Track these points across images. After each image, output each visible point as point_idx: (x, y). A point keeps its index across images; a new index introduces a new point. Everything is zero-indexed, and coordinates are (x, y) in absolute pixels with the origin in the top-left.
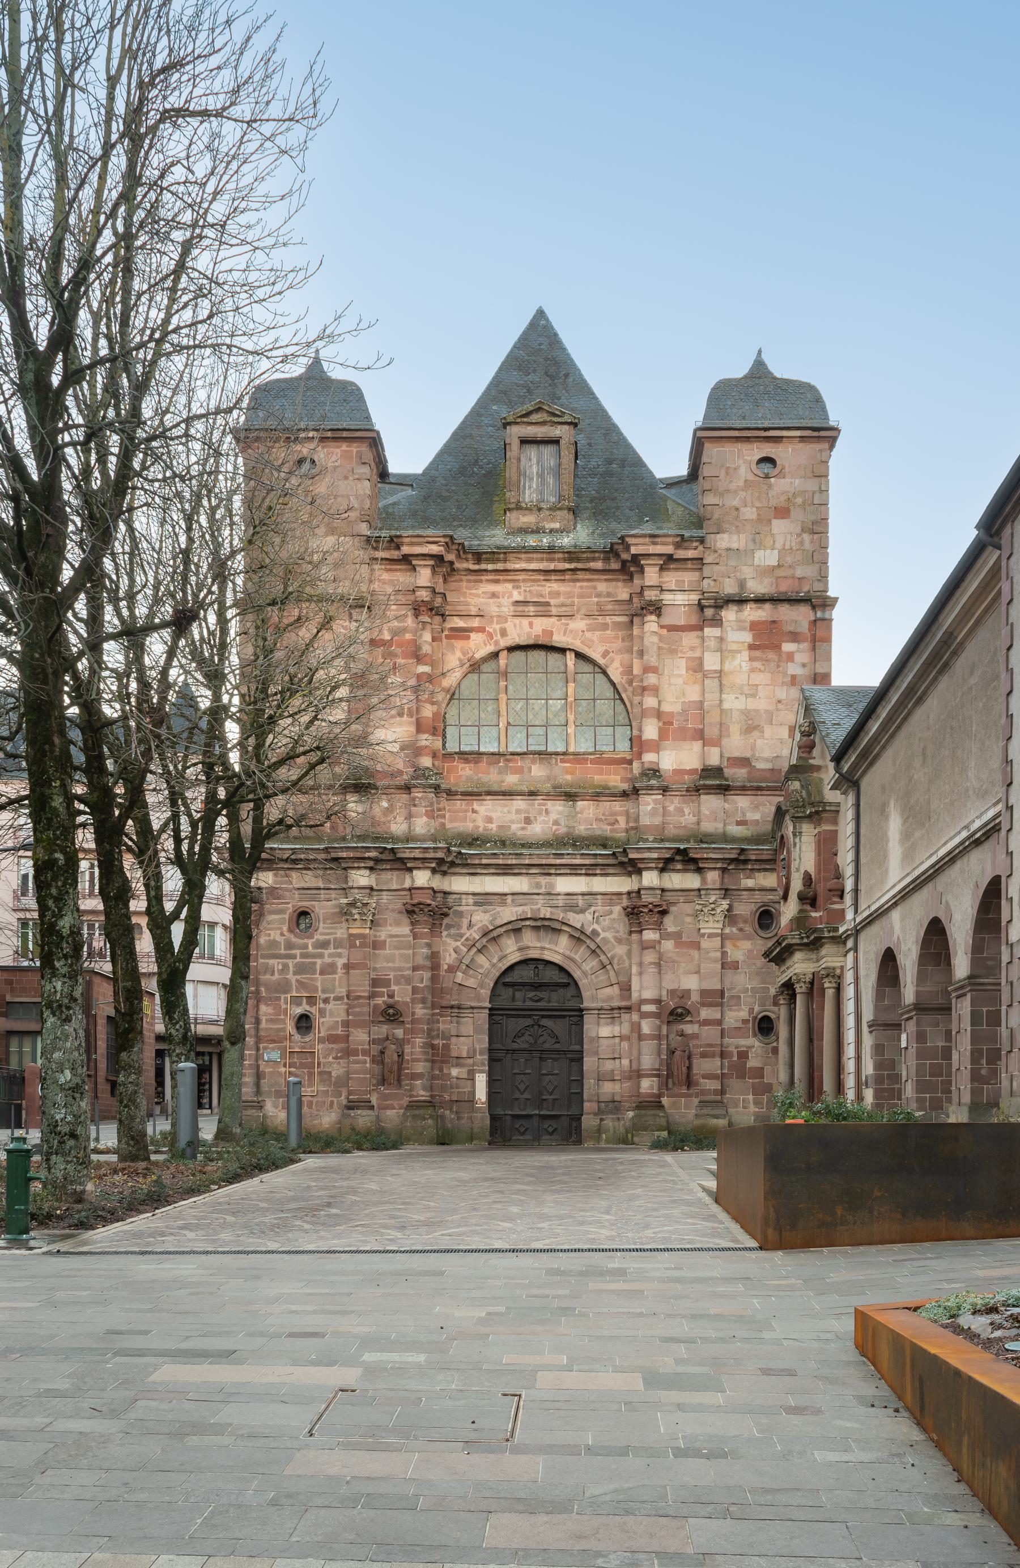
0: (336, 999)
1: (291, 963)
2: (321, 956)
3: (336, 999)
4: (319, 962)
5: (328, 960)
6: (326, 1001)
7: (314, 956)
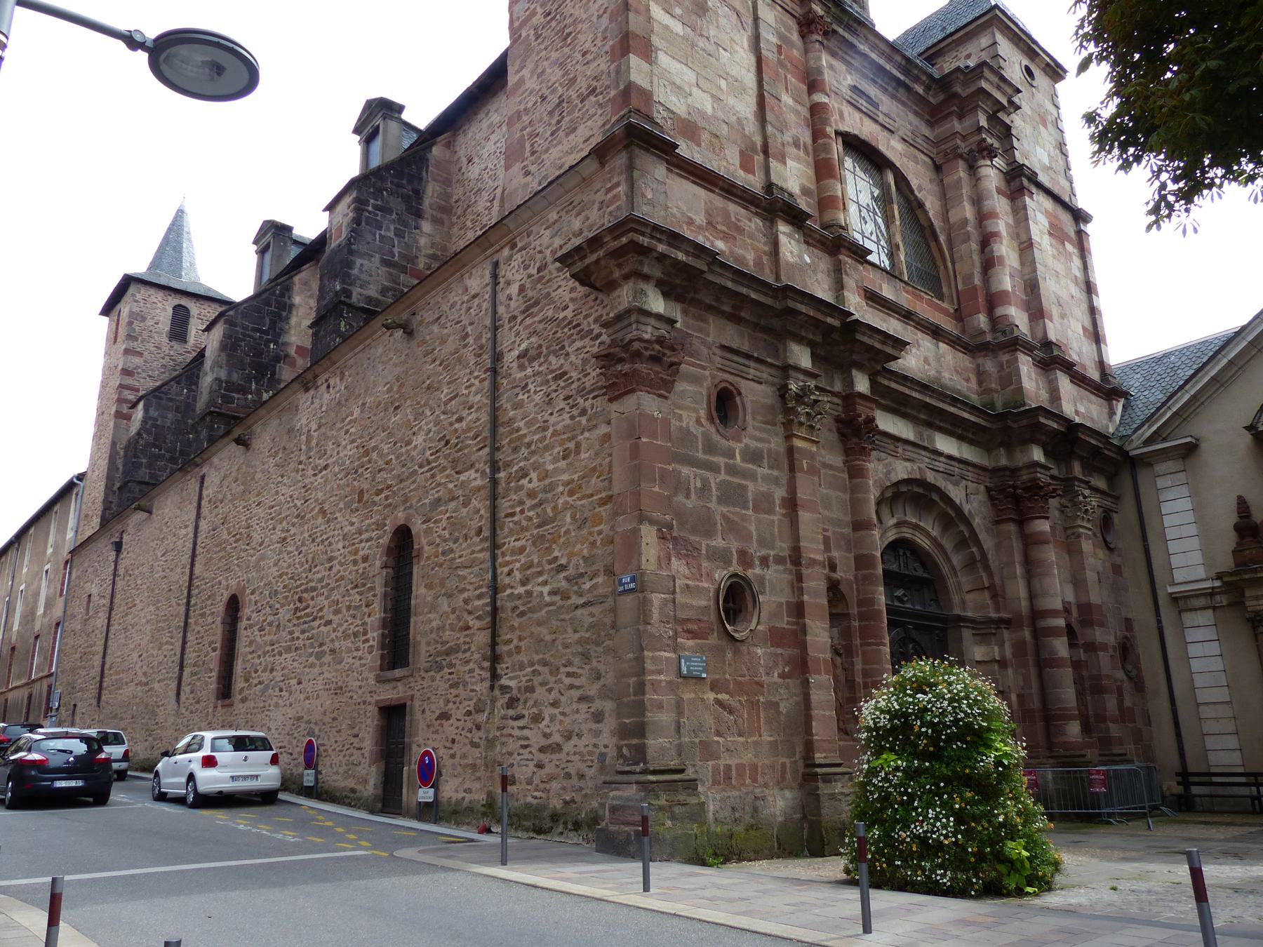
0: (779, 560)
2: (752, 476)
3: (779, 560)
4: (751, 486)
5: (763, 488)
6: (764, 561)
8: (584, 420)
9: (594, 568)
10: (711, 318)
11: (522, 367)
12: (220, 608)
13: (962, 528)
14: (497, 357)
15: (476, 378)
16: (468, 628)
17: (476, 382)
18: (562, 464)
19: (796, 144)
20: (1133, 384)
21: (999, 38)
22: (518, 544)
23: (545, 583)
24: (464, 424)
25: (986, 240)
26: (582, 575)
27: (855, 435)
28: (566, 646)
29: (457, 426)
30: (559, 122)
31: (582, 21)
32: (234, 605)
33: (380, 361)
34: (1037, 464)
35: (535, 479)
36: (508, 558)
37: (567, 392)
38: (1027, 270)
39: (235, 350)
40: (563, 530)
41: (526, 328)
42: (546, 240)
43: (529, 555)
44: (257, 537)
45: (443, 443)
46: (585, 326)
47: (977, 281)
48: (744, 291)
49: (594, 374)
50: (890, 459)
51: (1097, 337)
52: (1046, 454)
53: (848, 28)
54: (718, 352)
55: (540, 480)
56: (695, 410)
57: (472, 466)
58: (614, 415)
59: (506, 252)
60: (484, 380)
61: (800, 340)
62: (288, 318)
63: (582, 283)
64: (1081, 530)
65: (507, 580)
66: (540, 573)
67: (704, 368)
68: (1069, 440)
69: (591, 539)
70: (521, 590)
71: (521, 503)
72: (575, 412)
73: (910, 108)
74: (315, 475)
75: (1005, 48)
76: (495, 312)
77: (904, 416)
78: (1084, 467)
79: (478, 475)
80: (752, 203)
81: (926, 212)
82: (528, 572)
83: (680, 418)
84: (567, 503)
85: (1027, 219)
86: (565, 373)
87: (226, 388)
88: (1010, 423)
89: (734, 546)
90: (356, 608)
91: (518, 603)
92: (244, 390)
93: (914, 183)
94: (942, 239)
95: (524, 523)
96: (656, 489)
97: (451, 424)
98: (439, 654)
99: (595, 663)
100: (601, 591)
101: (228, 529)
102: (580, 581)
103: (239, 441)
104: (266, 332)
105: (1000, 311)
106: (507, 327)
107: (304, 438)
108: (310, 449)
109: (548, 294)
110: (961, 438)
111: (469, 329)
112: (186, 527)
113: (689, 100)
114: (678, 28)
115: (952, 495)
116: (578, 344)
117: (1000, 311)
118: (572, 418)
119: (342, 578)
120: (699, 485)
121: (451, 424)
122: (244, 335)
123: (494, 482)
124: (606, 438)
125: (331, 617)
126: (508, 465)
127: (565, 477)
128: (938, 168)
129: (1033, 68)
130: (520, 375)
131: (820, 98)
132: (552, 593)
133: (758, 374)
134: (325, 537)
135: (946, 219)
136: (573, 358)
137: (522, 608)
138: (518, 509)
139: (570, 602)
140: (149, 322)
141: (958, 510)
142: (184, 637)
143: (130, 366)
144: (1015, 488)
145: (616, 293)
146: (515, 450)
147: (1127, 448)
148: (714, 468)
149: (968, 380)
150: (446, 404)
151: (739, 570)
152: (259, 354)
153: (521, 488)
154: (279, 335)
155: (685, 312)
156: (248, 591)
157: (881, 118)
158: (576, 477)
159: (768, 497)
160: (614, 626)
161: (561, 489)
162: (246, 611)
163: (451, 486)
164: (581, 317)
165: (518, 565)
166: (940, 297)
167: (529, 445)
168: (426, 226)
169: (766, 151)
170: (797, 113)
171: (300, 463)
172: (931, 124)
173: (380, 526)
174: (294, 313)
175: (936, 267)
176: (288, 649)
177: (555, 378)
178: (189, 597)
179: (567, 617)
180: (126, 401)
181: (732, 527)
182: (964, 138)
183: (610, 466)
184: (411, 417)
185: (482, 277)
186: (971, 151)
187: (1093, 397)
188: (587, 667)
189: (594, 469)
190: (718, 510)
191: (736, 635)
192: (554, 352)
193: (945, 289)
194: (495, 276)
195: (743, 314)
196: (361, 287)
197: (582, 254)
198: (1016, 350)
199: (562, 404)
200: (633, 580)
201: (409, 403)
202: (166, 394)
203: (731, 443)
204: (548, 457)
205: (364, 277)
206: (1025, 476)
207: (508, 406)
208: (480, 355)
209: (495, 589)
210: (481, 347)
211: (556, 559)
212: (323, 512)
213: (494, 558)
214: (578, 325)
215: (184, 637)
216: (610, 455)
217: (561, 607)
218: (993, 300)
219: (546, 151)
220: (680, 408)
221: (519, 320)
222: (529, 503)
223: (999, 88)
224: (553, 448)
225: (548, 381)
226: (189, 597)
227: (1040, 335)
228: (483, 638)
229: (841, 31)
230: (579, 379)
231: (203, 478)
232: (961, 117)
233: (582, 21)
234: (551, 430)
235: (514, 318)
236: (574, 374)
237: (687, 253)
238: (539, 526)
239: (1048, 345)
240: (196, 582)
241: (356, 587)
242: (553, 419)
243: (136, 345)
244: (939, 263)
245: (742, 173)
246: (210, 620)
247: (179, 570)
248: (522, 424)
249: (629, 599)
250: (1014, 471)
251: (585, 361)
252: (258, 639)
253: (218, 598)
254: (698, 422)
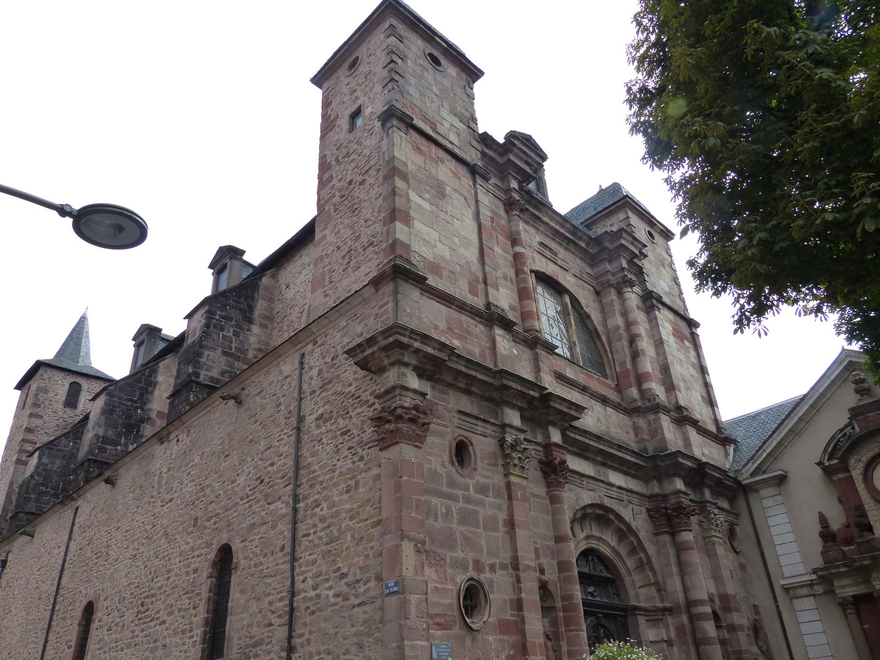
1: (455, 507)
3: (504, 567)
4: (481, 511)
5: (490, 512)
7: (477, 503)
8: (361, 464)
9: (368, 575)
10: (451, 392)
11: (318, 427)
12: (78, 613)
13: (632, 539)
14: (301, 419)
15: (285, 434)
16: (271, 625)
17: (285, 437)
18: (346, 497)
19: (505, 278)
20: (738, 434)
21: (630, 214)
22: (312, 557)
23: (331, 588)
24: (275, 467)
25: (633, 340)
26: (358, 581)
27: (553, 472)
28: (345, 639)
29: (270, 469)
30: (348, 263)
31: (365, 201)
32: (89, 610)
33: (217, 421)
34: (679, 492)
35: (325, 508)
36: (303, 569)
37: (350, 444)
38: (661, 358)
39: (112, 414)
40: (345, 546)
41: (322, 399)
42: (337, 339)
43: (319, 566)
45: (259, 481)
46: (363, 398)
47: (629, 366)
48: (473, 373)
49: (370, 430)
50: (579, 489)
51: (711, 401)
52: (686, 484)
53: (535, 207)
54: (456, 415)
55: (329, 509)
56: (441, 456)
57: (279, 498)
58: (383, 461)
59: (310, 347)
60: (291, 435)
61: (513, 406)
62: (152, 392)
63: (362, 368)
64: (715, 539)
65: (302, 586)
66: (327, 580)
67: (446, 426)
68: (699, 474)
69: (366, 553)
70: (312, 593)
71: (315, 526)
72: (356, 458)
73: (577, 256)
74: (162, 506)
75: (634, 220)
76: (301, 388)
77: (586, 458)
78: (712, 493)
79: (284, 505)
80: (477, 315)
81: (592, 321)
82: (318, 579)
83: (430, 463)
84: (348, 525)
85: (658, 325)
86: (349, 431)
87: (102, 442)
88: (659, 463)
89: (470, 556)
90: (186, 610)
91: (309, 604)
92: (115, 443)
93: (583, 303)
94: (604, 338)
95: (316, 541)
96: (413, 514)
97: (266, 468)
98: (248, 646)
99: (367, 652)
100: (372, 593)
101: (92, 548)
102: (357, 586)
103: (108, 481)
104: (136, 402)
105: (645, 386)
106: (309, 398)
107: (156, 478)
108: (160, 487)
109: (338, 375)
110: (626, 474)
111: (282, 400)
112: (59, 547)
113: (435, 250)
114: (427, 206)
115: (623, 515)
116: (359, 410)
117: (645, 386)
118: (353, 463)
119: (177, 586)
120: (444, 511)
121: (266, 468)
122: (120, 403)
123: (295, 510)
124: (378, 477)
125: (166, 618)
126: (305, 498)
127: (347, 506)
128: (598, 293)
129: (652, 232)
130: (317, 432)
131: (519, 249)
132: (336, 596)
133: (484, 430)
134: (166, 554)
135: (605, 326)
136: (354, 420)
137: (312, 608)
138: (312, 531)
139: (349, 602)
140: (51, 394)
141: (629, 526)
142: (47, 637)
143: (32, 426)
144: (666, 509)
145: (385, 375)
146: (312, 486)
147: (740, 479)
148: (454, 498)
149: (628, 433)
150: (262, 453)
151: (475, 575)
152: (129, 417)
153: (314, 515)
154: (145, 404)
155: (433, 388)
156: (102, 598)
157: (559, 262)
158: (355, 506)
159: (494, 519)
160: (382, 621)
161: (344, 515)
162: (98, 615)
163: (263, 513)
164: (361, 391)
165: (310, 574)
166: (605, 376)
167: (322, 483)
168: (255, 329)
169: (485, 282)
170: (505, 259)
171: (152, 497)
172: (592, 266)
173: (209, 545)
174: (158, 388)
175: (601, 357)
176: (129, 646)
177: (342, 434)
179: (347, 615)
180: (26, 451)
181: (468, 541)
182: (613, 274)
183: (380, 498)
184: (237, 463)
185: (293, 364)
186: (618, 283)
187: (713, 444)
188: (361, 655)
189: (368, 500)
190: (459, 530)
191: (473, 626)
192: (342, 416)
193: (608, 372)
194: (302, 363)
195: (473, 389)
196: (207, 370)
197: (362, 349)
198: (659, 412)
199: (346, 453)
200: (396, 584)
201: (235, 452)
202: (57, 446)
203: (467, 480)
204: (335, 491)
205: (209, 363)
206: (673, 500)
207: (307, 454)
208: (289, 418)
209: (293, 593)
210: (290, 412)
211: (339, 568)
212: (166, 534)
213: (293, 569)
214: (359, 397)
215: (47, 637)
216: (380, 490)
217: (343, 606)
218: (640, 379)
219: (340, 281)
220: (430, 455)
221: (317, 393)
222: (321, 526)
223: (633, 244)
224: (339, 484)
225: (337, 436)
227: (673, 402)
228: (283, 632)
229: (531, 209)
230: (359, 435)
231: (77, 509)
232: (610, 261)
233: (365, 201)
234: (338, 472)
235: (314, 392)
236: (355, 432)
237: (434, 348)
238: (327, 544)
239: (679, 408)
240: (62, 592)
241: (187, 593)
242: (339, 464)
243: (40, 411)
244: (603, 354)
245: (470, 296)
246: (69, 622)
247: (49, 582)
248: (317, 467)
249: (393, 599)
250: (664, 497)
251: (363, 422)
252: (106, 637)
253: (78, 605)
254: (443, 465)
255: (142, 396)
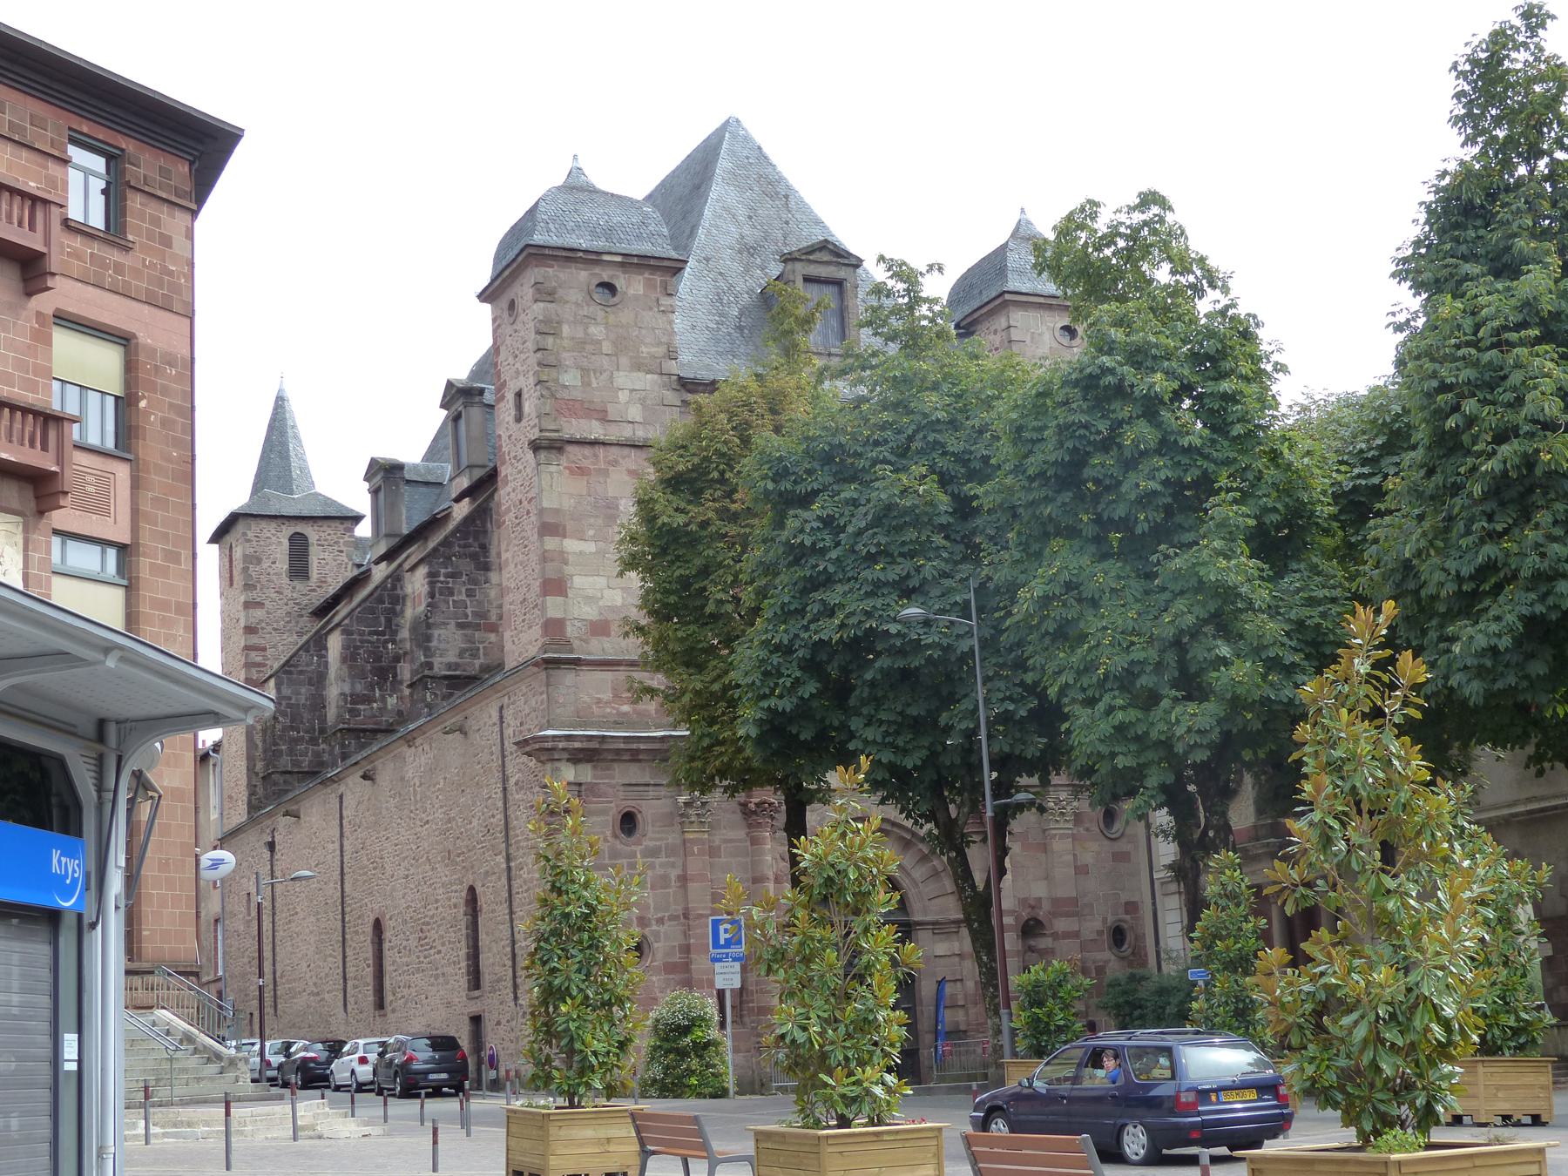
0: (673, 918)
3: (673, 918)
12: (369, 929)
32: (378, 926)
44: (389, 871)
62: (402, 611)
123: (509, 869)
162: (387, 935)
178: (343, 913)
205: (442, 646)
226: (343, 913)
255: (389, 621)
